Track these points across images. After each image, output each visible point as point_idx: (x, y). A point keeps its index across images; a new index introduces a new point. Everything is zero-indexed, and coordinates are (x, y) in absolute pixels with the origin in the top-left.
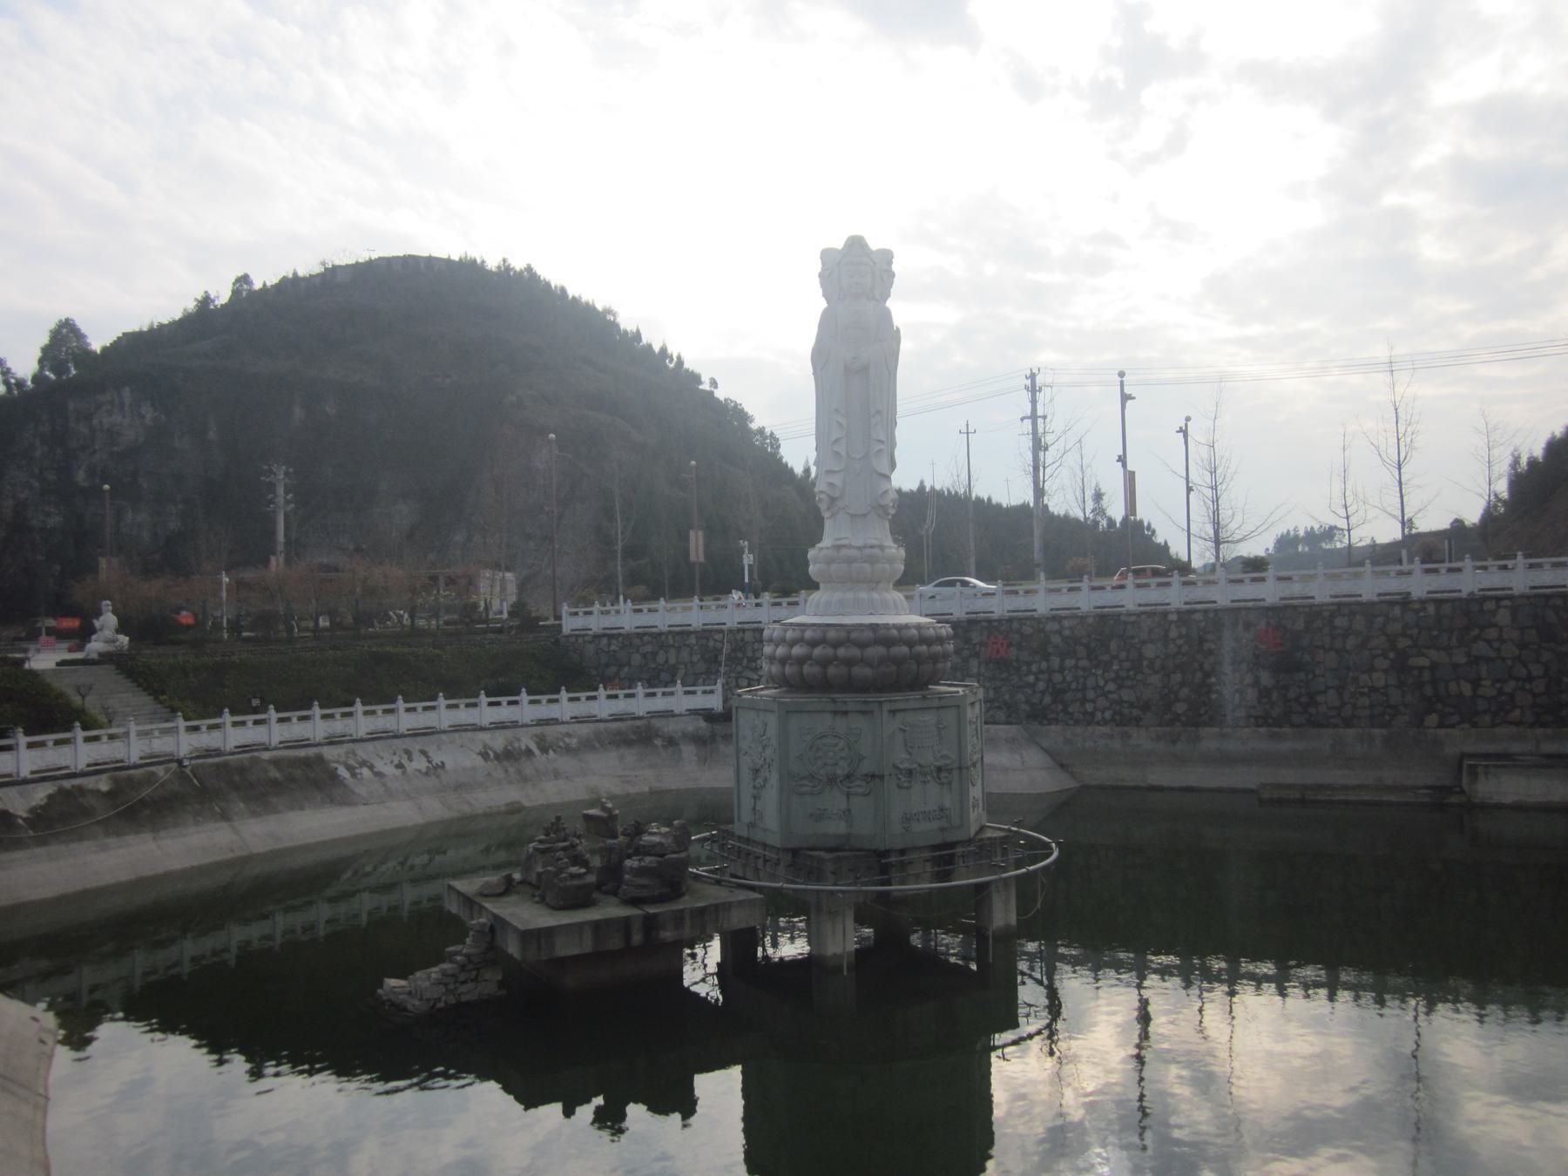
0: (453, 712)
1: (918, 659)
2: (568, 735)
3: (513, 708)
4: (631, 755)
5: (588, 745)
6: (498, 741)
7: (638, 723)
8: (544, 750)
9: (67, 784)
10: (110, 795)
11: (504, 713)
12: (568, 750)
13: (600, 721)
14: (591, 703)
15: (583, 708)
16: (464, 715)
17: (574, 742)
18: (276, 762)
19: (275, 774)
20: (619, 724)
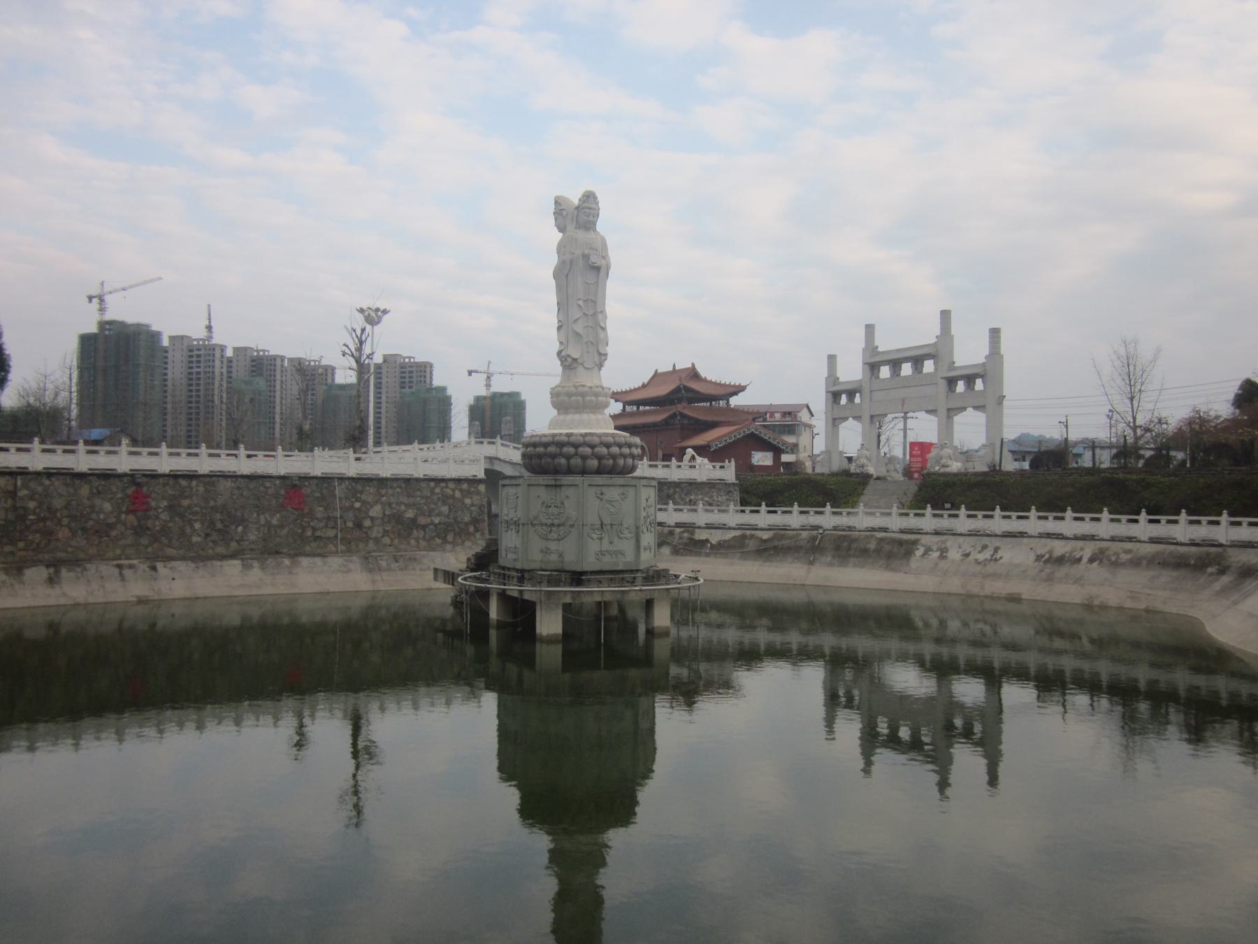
0: (1042, 522)
1: (614, 457)
2: (1129, 551)
3: (1094, 523)
4: (1166, 575)
5: (1136, 563)
6: (1060, 548)
7: (1213, 550)
8: (1091, 560)
9: (748, 533)
10: (765, 541)
11: (1086, 527)
12: (1116, 564)
13: (1177, 544)
14: (1171, 526)
15: (1161, 530)
16: (1051, 525)
17: (1124, 557)
18: (881, 540)
19: (872, 546)
20: (1193, 549)
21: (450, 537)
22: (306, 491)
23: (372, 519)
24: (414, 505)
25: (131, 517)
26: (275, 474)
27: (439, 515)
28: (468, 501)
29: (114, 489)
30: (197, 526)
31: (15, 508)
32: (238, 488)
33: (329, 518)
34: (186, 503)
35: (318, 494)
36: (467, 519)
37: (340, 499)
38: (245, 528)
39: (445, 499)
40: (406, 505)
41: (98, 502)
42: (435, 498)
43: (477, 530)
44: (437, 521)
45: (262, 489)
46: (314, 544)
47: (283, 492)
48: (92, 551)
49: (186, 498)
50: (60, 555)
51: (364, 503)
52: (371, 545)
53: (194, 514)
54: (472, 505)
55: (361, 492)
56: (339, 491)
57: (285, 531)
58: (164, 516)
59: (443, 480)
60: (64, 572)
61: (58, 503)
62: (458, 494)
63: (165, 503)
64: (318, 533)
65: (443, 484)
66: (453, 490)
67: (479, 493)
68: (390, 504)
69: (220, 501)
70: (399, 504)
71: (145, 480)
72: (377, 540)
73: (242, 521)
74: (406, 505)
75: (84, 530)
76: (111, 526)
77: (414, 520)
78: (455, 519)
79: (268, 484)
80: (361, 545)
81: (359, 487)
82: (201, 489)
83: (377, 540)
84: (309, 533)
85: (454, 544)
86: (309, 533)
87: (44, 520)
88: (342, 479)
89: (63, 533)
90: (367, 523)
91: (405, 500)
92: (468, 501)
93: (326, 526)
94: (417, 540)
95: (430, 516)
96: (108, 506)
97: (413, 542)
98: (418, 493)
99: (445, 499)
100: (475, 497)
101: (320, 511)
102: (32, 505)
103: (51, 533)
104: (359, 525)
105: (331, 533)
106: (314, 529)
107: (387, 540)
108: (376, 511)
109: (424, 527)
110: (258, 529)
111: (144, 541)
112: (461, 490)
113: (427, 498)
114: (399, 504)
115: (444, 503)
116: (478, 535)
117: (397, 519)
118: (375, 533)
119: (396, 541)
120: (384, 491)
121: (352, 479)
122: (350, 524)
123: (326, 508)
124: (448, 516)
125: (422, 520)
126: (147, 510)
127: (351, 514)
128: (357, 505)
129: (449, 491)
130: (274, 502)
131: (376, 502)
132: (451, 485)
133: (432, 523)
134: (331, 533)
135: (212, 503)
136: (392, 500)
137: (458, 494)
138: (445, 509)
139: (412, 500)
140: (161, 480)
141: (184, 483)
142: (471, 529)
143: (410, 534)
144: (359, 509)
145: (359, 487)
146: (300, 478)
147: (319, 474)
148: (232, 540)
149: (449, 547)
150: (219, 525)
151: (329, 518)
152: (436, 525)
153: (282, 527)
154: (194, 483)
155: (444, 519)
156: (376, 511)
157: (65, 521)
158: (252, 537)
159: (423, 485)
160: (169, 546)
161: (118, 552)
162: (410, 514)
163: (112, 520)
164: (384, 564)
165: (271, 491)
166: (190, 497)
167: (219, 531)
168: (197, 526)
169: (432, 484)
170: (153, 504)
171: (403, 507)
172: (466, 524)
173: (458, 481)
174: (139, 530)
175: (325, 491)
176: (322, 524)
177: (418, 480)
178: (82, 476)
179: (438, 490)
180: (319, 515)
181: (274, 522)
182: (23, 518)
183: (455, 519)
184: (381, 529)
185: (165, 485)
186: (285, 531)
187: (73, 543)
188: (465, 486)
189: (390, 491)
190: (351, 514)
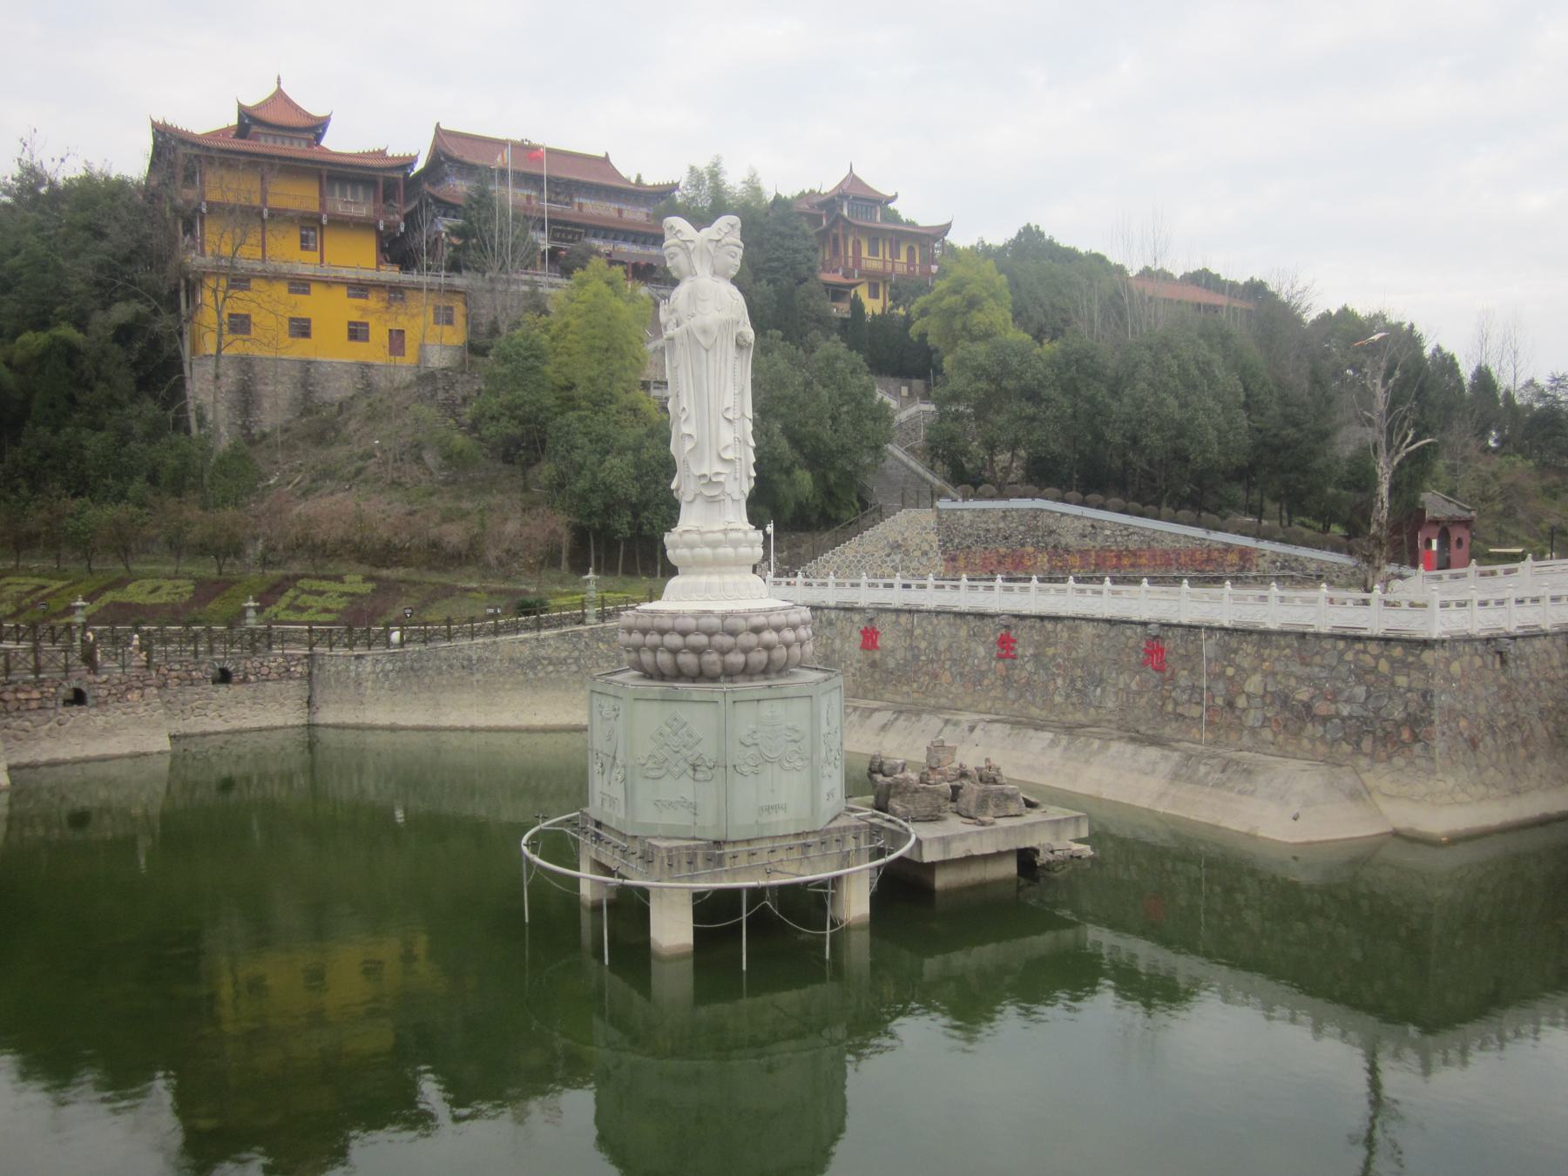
21: (1367, 744)
22: (1168, 645)
23: (1249, 696)
24: (1309, 678)
25: (1000, 665)
26: (1136, 618)
27: (1349, 701)
28: (1401, 681)
29: (987, 630)
30: (1060, 682)
31: (912, 648)
32: (1099, 636)
33: (1193, 687)
34: (1050, 651)
35: (1182, 651)
36: (1398, 714)
37: (1209, 660)
38: (1103, 690)
39: (1361, 673)
40: (1299, 679)
41: (973, 645)
42: (1343, 669)
43: (1415, 738)
44: (1345, 713)
45: (1123, 639)
46: (1174, 725)
47: (1143, 645)
48: (968, 700)
49: (1050, 645)
50: (943, 701)
51: (1239, 668)
52: (1246, 740)
53: (1058, 666)
54: (1409, 690)
55: (1235, 652)
56: (1208, 647)
57: (1144, 700)
58: (1030, 667)
59: (1358, 639)
60: (901, 723)
61: (943, 644)
62: (1384, 666)
63: (1031, 651)
64: (1180, 710)
65: (1359, 646)
66: (1376, 658)
67: (1423, 667)
68: (1274, 674)
69: (1081, 653)
70: (1288, 675)
71: (1014, 621)
72: (1253, 731)
73: (1100, 681)
74: (1299, 679)
75: (961, 674)
76: (983, 674)
77: (1308, 707)
78: (1377, 711)
79: (1129, 632)
80: (1233, 737)
81: (1234, 644)
82: (1065, 635)
83: (1253, 731)
84: (1170, 708)
85: (1372, 756)
86: (1170, 708)
87: (932, 661)
88: (1211, 629)
89: (946, 677)
90: (1241, 702)
91: (1296, 669)
92: (1401, 681)
93: (1189, 701)
94: (1312, 740)
95: (1334, 701)
96: (981, 651)
97: (1305, 742)
98: (1317, 659)
99: (1361, 673)
100: (1415, 674)
101: (1183, 678)
102: (923, 645)
103: (935, 676)
104: (1231, 704)
105: (1195, 711)
106: (1176, 704)
107: (1267, 734)
108: (1254, 684)
109: (1325, 720)
110: (1116, 694)
111: (1011, 695)
112: (1392, 661)
113: (1333, 669)
114: (1288, 675)
115: (1359, 683)
116: (1418, 748)
117: (1285, 700)
118: (1253, 718)
119: (1281, 738)
120: (1267, 652)
121: (1226, 629)
122: (1219, 701)
123: (1192, 671)
124: (1364, 705)
125: (1322, 708)
126: (1014, 657)
127: (1220, 686)
128: (1230, 671)
129: (1368, 660)
130: (1133, 659)
131: (1255, 670)
132: (1373, 648)
133: (1338, 715)
134: (1195, 711)
135: (1074, 654)
136: (1279, 667)
137: (1384, 666)
138: (1360, 691)
139: (1308, 670)
140: (1028, 622)
141: (1049, 626)
142: (1406, 735)
143: (1301, 729)
144: (1231, 679)
145: (1234, 644)
146: (1163, 625)
147: (1185, 621)
148: (1090, 704)
149: (1363, 762)
150: (1079, 685)
151: (1193, 687)
152: (1343, 719)
153: (1139, 693)
154: (1060, 626)
155: (1359, 711)
156: (1254, 684)
157: (948, 664)
158: (1110, 705)
159: (1327, 644)
160: (1033, 704)
161: (989, 704)
162: (1303, 694)
163: (984, 668)
164: (1203, 769)
165: (1131, 643)
166: (1055, 644)
167: (1079, 691)
168: (1060, 682)
169: (1341, 645)
170: (1020, 651)
171: (1293, 682)
172: (1398, 725)
173: (1386, 641)
174: (1007, 681)
175: (1190, 647)
176: (1185, 697)
177: (1317, 636)
178: (961, 615)
179: (1349, 656)
180: (1183, 682)
181: (1134, 686)
182: (916, 658)
183: (1377, 711)
184: (1259, 714)
185: (1031, 628)
186: (1144, 700)
187: (953, 689)
188: (1397, 652)
189: (1275, 653)
190: (1221, 685)
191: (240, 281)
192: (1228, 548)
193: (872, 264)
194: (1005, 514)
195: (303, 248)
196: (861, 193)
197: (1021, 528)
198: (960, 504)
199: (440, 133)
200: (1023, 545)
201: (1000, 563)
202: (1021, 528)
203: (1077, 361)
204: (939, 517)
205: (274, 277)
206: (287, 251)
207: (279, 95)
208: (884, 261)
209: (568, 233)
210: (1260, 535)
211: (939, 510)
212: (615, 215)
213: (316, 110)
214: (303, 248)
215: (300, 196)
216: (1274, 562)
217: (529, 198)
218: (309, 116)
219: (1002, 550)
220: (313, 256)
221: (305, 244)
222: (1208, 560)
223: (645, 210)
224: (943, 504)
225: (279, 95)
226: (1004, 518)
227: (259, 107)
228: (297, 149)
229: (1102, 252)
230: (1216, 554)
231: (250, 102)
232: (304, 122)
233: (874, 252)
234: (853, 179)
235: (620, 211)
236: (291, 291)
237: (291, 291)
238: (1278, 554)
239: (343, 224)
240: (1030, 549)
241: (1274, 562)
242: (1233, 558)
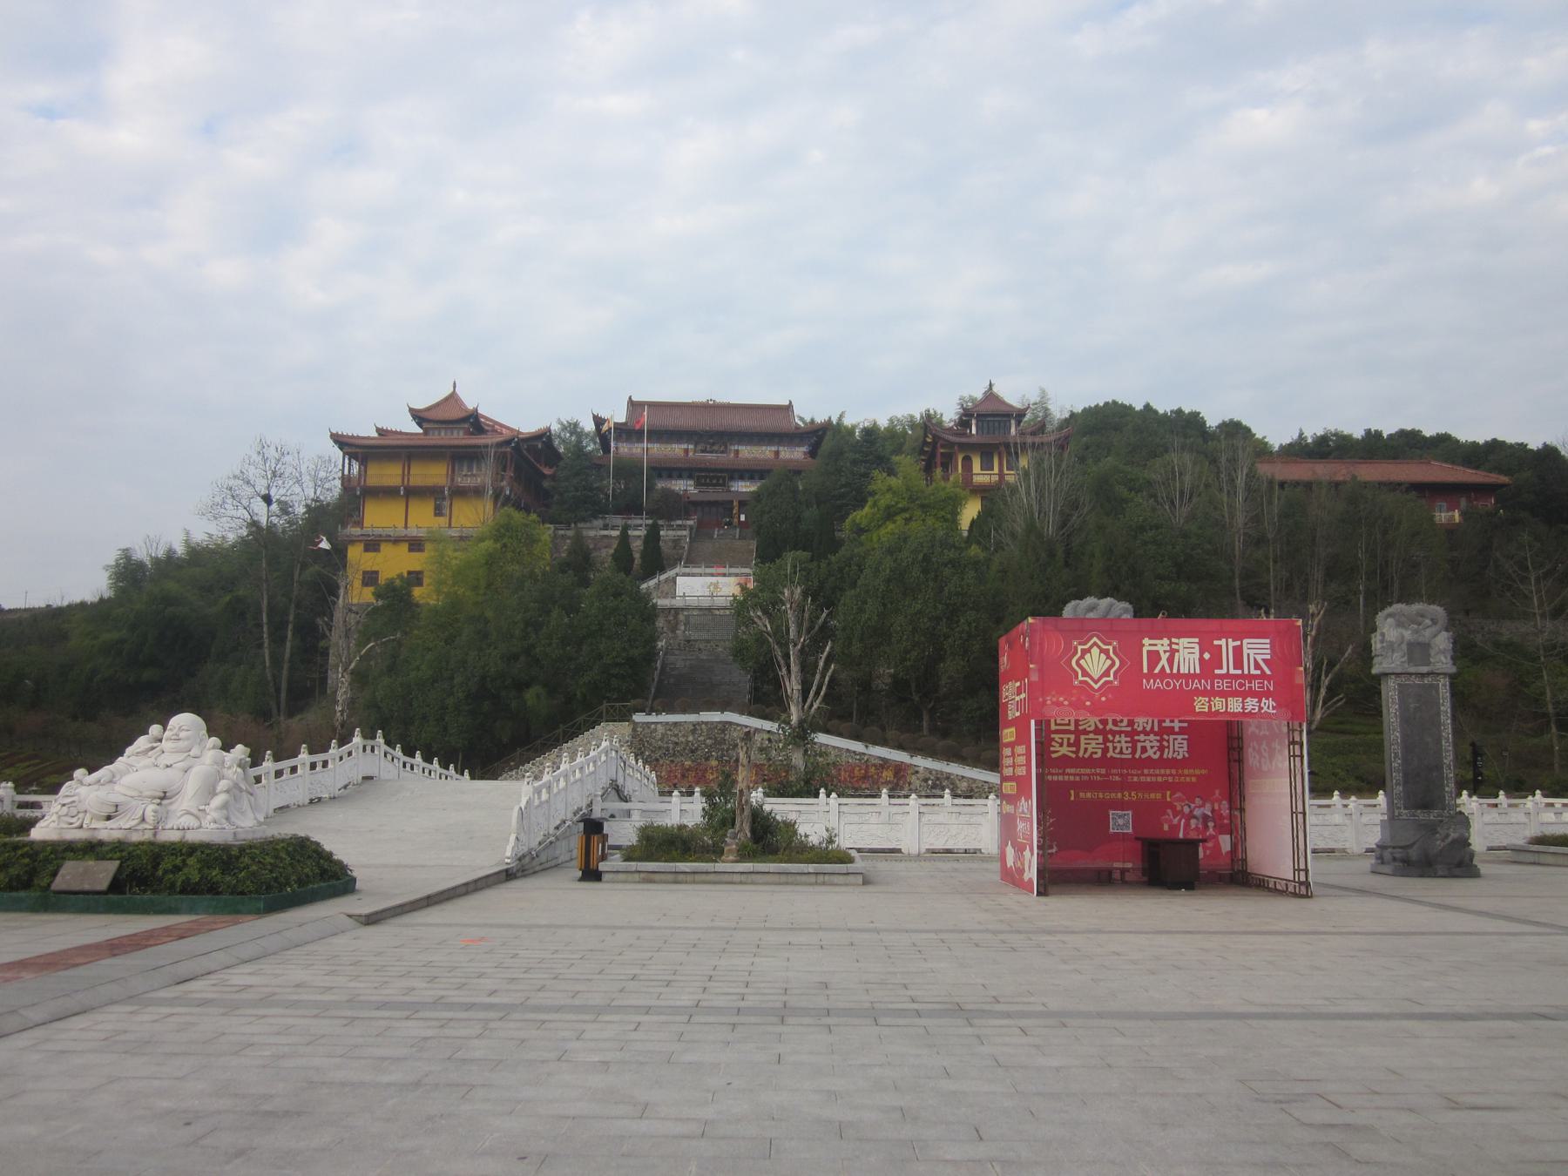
191: (372, 545)
192: (885, 763)
193: (981, 476)
194: (695, 725)
195: (436, 515)
196: (990, 408)
197: (709, 742)
198: (653, 718)
199: (634, 406)
200: (707, 759)
201: (683, 776)
202: (709, 742)
203: (841, 570)
204: (634, 730)
205: (397, 541)
206: (422, 518)
207: (453, 398)
208: (1001, 475)
209: (711, 478)
210: (915, 750)
211: (635, 724)
212: (772, 456)
213: (471, 407)
214: (436, 515)
215: (434, 474)
216: (926, 780)
217: (686, 451)
218: (466, 410)
219: (688, 763)
220: (443, 521)
221: (438, 512)
222: (865, 777)
223: (804, 449)
224: (639, 718)
225: (453, 398)
226: (694, 731)
227: (428, 409)
228: (458, 438)
229: (1442, 429)
230: (873, 770)
231: (420, 405)
232: (463, 414)
233: (987, 466)
234: (990, 395)
235: (777, 453)
236: (411, 550)
237: (411, 550)
238: (930, 771)
239: (460, 493)
240: (714, 763)
241: (926, 780)
242: (888, 775)
